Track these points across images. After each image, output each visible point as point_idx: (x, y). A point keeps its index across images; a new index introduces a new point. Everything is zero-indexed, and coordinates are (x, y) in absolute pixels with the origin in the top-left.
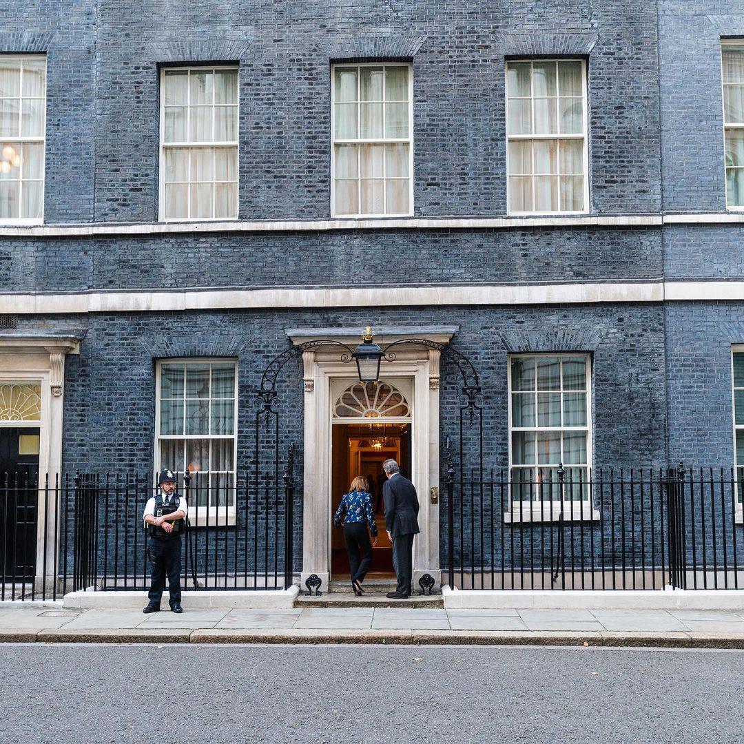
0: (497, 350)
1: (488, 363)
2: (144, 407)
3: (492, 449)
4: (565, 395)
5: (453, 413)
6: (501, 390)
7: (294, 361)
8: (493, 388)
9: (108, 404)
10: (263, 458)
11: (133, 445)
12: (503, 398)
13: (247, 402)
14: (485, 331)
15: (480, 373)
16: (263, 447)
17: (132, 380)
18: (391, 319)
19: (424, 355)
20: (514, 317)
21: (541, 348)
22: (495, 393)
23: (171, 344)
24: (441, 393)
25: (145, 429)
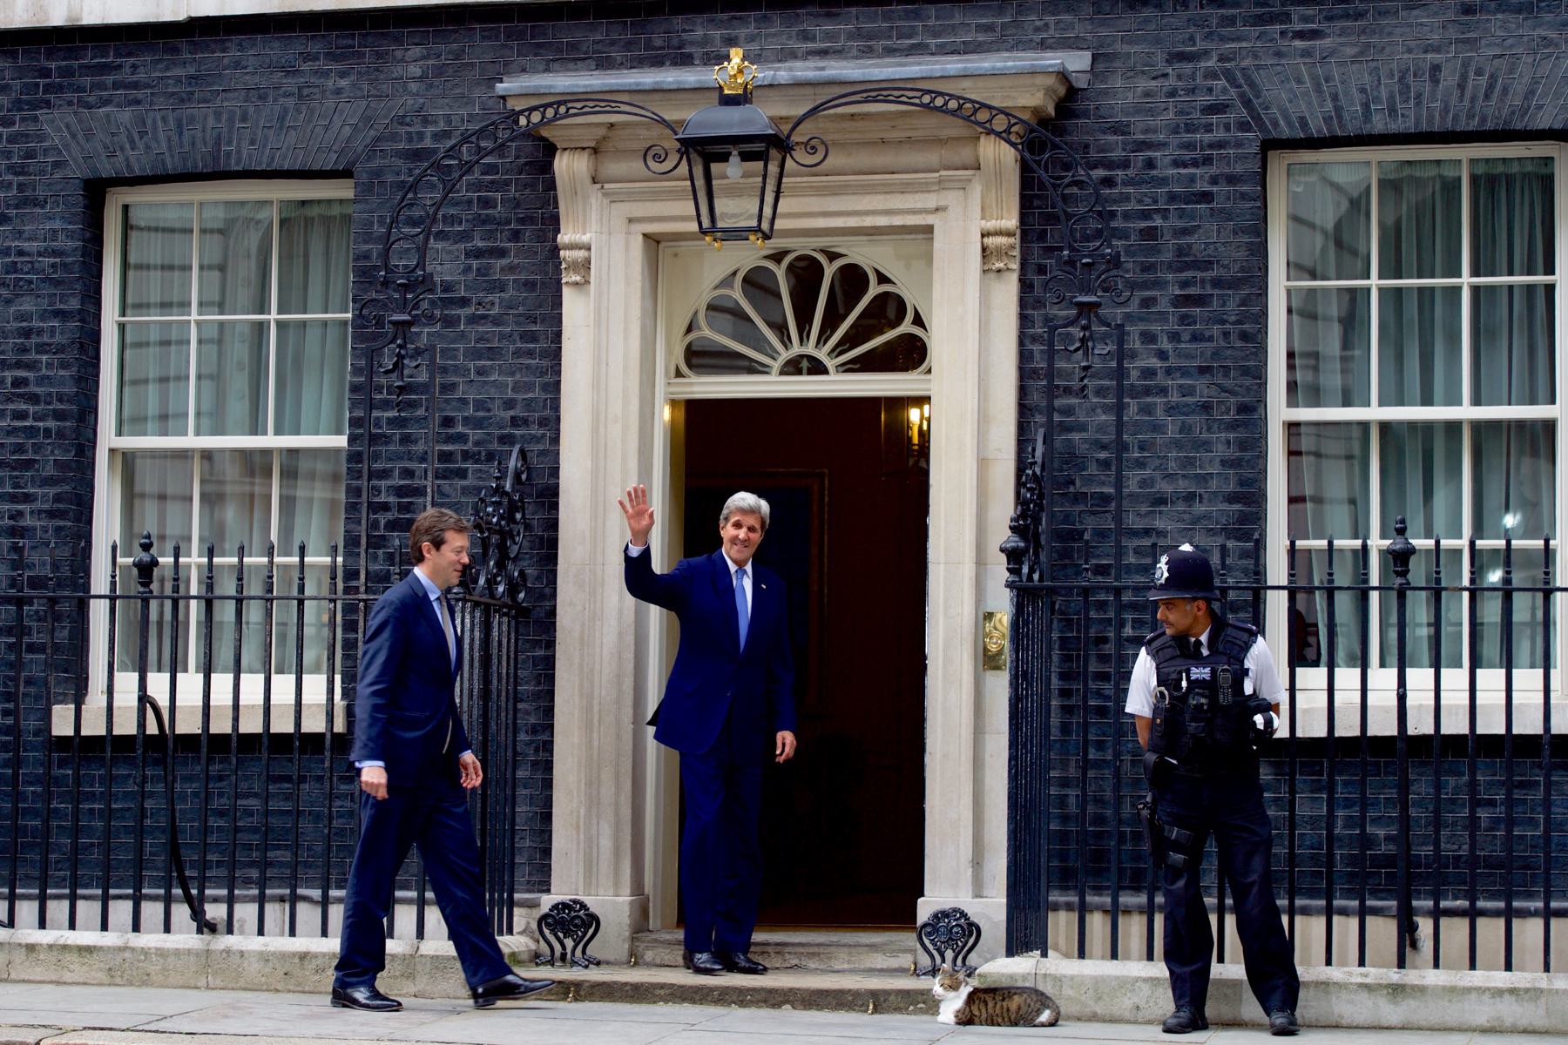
0: (1219, 134)
1: (1192, 179)
2: (58, 339)
3: (1204, 479)
4: (1476, 290)
6: (1234, 271)
7: (533, 186)
8: (1207, 265)
12: (1243, 303)
14: (1187, 67)
15: (1165, 214)
17: (21, 253)
18: (858, 34)
19: (965, 154)
20: (1285, 18)
21: (1379, 125)
22: (1217, 283)
23: (142, 134)
24: (1025, 286)
25: (59, 415)
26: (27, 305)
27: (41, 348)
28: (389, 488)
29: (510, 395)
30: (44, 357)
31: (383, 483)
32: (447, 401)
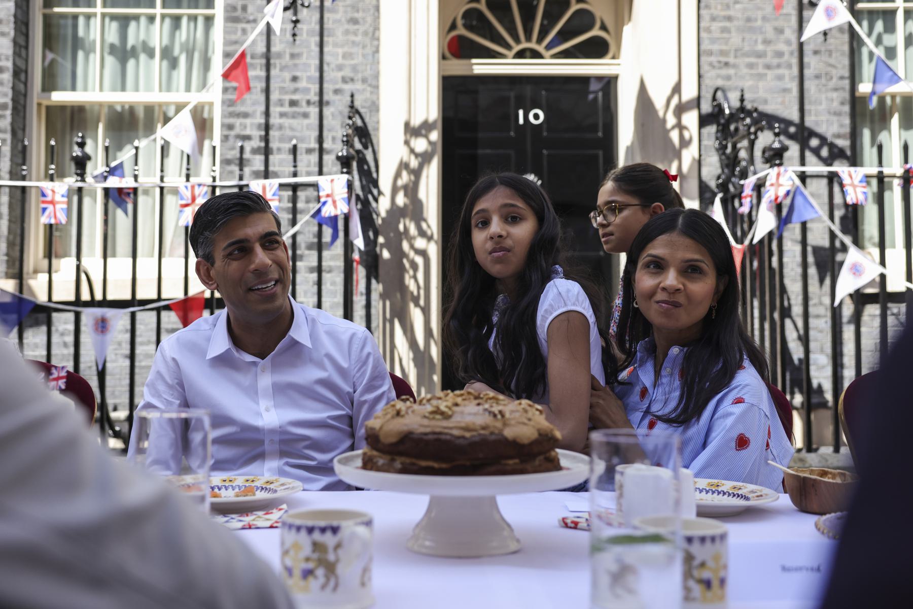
5: (727, 41)
10: (281, 140)
16: (282, 115)
28: (252, 124)
29: (340, 61)
31: (248, 121)
32: (295, 65)
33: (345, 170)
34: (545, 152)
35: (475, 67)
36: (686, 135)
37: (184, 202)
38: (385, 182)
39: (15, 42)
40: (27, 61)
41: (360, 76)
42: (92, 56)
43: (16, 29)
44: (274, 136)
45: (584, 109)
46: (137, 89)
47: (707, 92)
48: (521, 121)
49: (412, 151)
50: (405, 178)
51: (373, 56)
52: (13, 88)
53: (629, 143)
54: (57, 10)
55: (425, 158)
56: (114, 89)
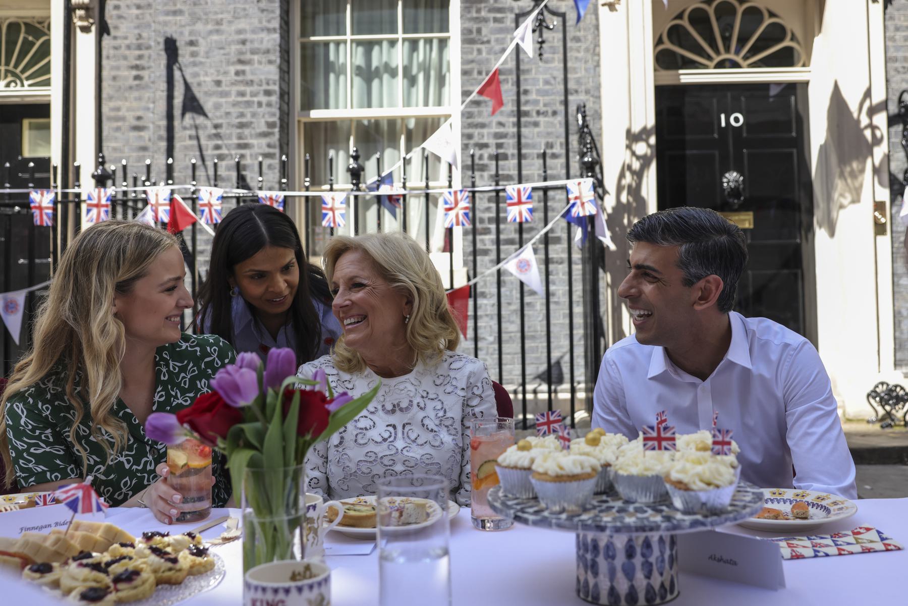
9: (192, 43)
11: (242, 126)
13: (479, 31)
25: (268, 93)
26: (242, 24)
27: (254, 52)
28: (489, 134)
30: (256, 57)
31: (485, 131)
33: (590, 174)
34: (745, 151)
35: (682, 77)
36: (878, 133)
37: (448, 206)
38: (610, 183)
39: (280, 68)
40: (289, 84)
41: (583, 88)
42: (342, 78)
43: (282, 57)
44: (508, 144)
45: (781, 112)
46: (381, 106)
47: (894, 95)
48: (723, 124)
49: (633, 153)
50: (628, 179)
51: (595, 70)
52: (280, 109)
53: (822, 142)
54: (313, 38)
55: (645, 161)
56: (361, 107)
